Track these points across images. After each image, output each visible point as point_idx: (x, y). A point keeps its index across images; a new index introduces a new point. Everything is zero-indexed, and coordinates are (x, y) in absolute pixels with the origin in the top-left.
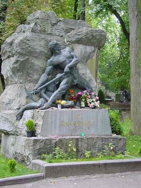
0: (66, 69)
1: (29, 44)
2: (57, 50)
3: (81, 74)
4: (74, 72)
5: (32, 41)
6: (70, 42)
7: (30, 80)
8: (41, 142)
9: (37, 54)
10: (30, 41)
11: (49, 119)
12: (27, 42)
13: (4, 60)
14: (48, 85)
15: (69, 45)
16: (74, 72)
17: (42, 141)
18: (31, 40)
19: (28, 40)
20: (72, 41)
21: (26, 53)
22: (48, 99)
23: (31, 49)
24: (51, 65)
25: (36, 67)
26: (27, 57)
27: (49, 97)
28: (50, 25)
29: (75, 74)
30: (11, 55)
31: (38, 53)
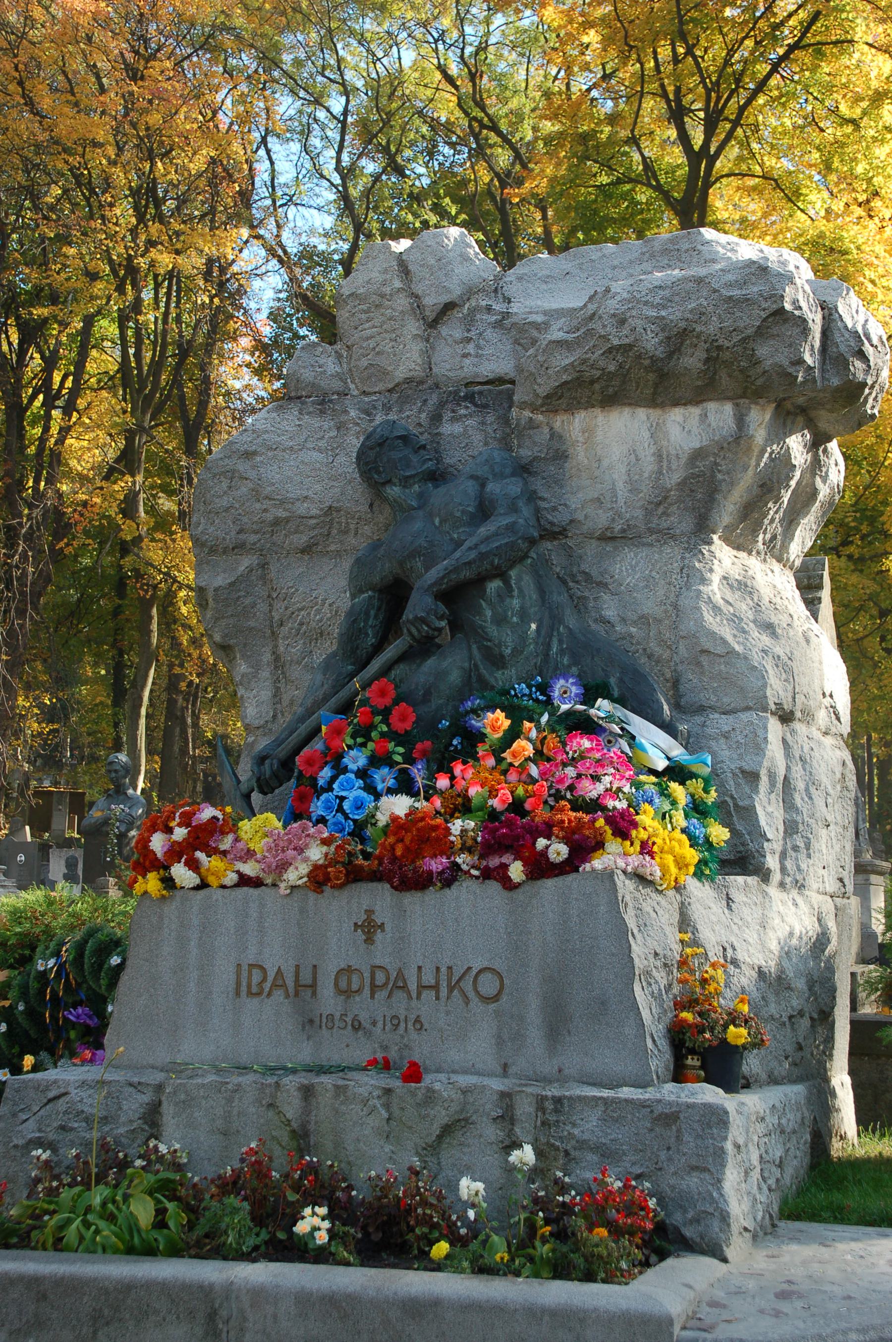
0: (420, 604)
1: (252, 474)
2: (389, 482)
3: (623, 620)
4: (489, 613)
5: (270, 454)
6: (534, 409)
8: (50, 1101)
10: (258, 459)
15: (531, 432)
16: (489, 613)
18: (270, 449)
19: (248, 455)
20: (540, 402)
21: (242, 537)
23: (267, 504)
24: (361, 591)
26: (246, 562)
28: (413, 327)
29: (493, 630)
31: (314, 521)
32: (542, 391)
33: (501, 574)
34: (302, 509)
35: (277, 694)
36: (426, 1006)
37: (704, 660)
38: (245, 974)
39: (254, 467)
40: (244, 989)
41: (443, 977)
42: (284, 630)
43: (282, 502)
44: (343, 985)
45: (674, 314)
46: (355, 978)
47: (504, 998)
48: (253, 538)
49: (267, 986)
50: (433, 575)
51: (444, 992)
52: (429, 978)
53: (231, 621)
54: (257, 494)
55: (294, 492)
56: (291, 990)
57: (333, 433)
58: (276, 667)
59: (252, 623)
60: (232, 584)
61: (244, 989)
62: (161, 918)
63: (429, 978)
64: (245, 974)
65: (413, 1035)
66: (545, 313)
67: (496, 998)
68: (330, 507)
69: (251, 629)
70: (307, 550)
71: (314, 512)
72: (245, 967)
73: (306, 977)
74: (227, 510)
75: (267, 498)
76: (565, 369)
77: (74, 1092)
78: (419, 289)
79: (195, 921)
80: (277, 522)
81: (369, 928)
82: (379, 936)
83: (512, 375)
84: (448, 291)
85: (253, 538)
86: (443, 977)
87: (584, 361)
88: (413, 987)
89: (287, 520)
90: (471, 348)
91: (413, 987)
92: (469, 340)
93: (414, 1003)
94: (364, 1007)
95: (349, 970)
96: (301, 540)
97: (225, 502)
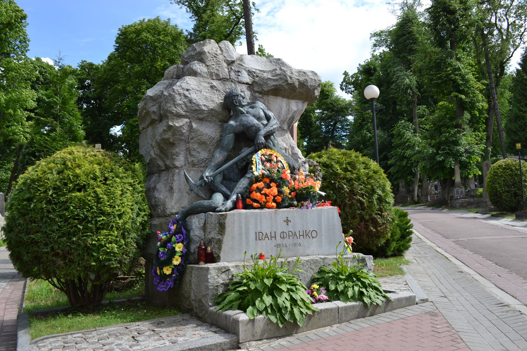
6: (260, 93)
7: (193, 161)
9: (205, 114)
11: (236, 229)
12: (186, 93)
13: (143, 130)
14: (227, 169)
17: (225, 271)
19: (188, 90)
22: (229, 193)
24: (230, 133)
25: (204, 138)
27: (231, 190)
28: (225, 65)
30: (156, 118)
32: (266, 89)
33: (272, 134)
34: (204, 108)
35: (186, 158)
36: (301, 240)
37: (299, 159)
38: (258, 235)
39: (189, 94)
40: (258, 238)
41: (305, 233)
42: (192, 141)
43: (198, 105)
44: (282, 236)
45: (302, 79)
46: (285, 234)
47: (317, 237)
48: (188, 114)
49: (263, 237)
50: (263, 132)
51: (305, 236)
52: (301, 234)
53: (178, 136)
54: (191, 101)
55: (201, 103)
56: (270, 239)
57: (209, 88)
58: (187, 151)
59: (183, 138)
60: (181, 126)
61: (258, 238)
62: (234, 220)
63: (301, 234)
64: (258, 235)
65: (299, 247)
66: (256, 70)
67: (316, 237)
68: (212, 109)
69: (182, 139)
70: (201, 120)
71: (207, 109)
72: (258, 234)
73: (273, 235)
74: (181, 104)
75: (194, 103)
76: (274, 86)
77: (232, 269)
78: (225, 55)
79: (243, 221)
80: (196, 110)
81: (287, 221)
82: (290, 223)
83: (250, 83)
84: (233, 58)
85: (188, 114)
86: (305, 233)
87: (280, 85)
88: (298, 236)
89: (198, 110)
90: (240, 74)
91: (298, 236)
92: (239, 72)
93: (299, 239)
94: (286, 241)
95: (283, 232)
96: (201, 116)
97: (180, 102)
